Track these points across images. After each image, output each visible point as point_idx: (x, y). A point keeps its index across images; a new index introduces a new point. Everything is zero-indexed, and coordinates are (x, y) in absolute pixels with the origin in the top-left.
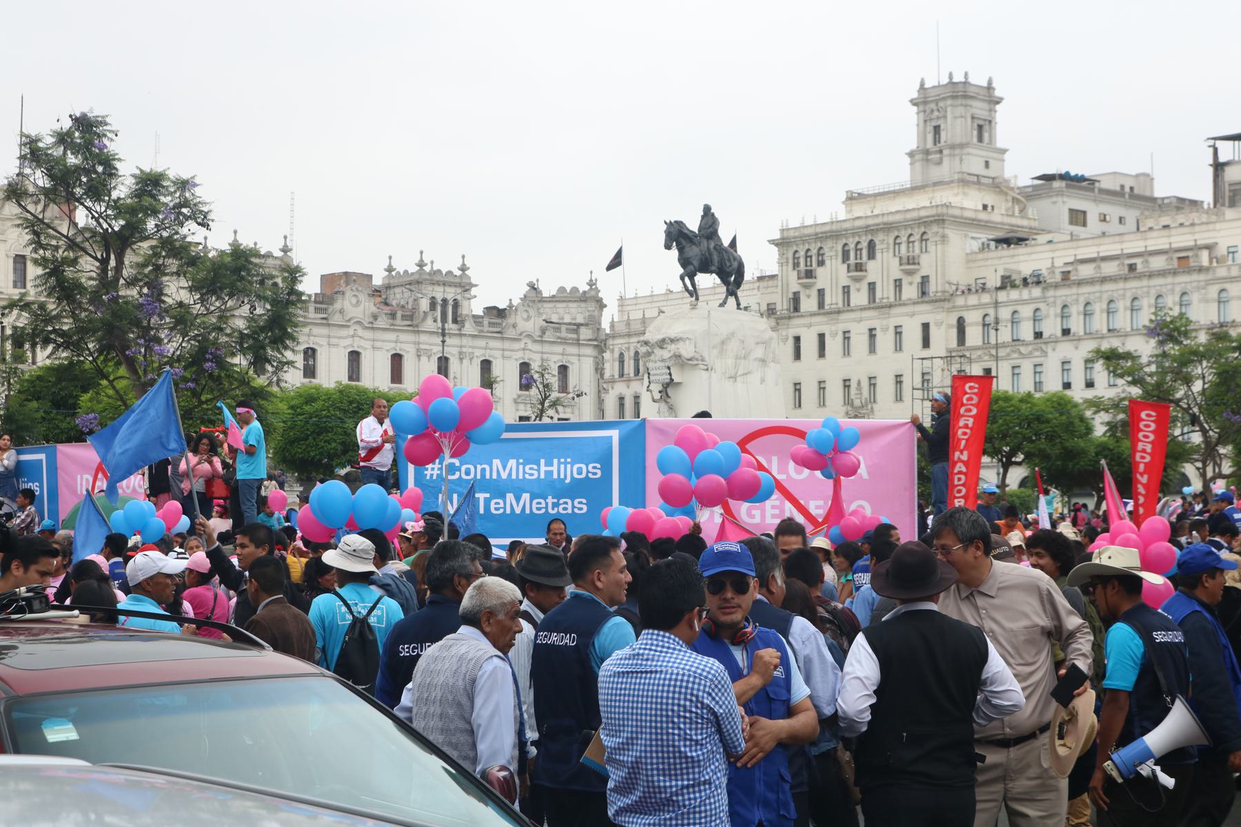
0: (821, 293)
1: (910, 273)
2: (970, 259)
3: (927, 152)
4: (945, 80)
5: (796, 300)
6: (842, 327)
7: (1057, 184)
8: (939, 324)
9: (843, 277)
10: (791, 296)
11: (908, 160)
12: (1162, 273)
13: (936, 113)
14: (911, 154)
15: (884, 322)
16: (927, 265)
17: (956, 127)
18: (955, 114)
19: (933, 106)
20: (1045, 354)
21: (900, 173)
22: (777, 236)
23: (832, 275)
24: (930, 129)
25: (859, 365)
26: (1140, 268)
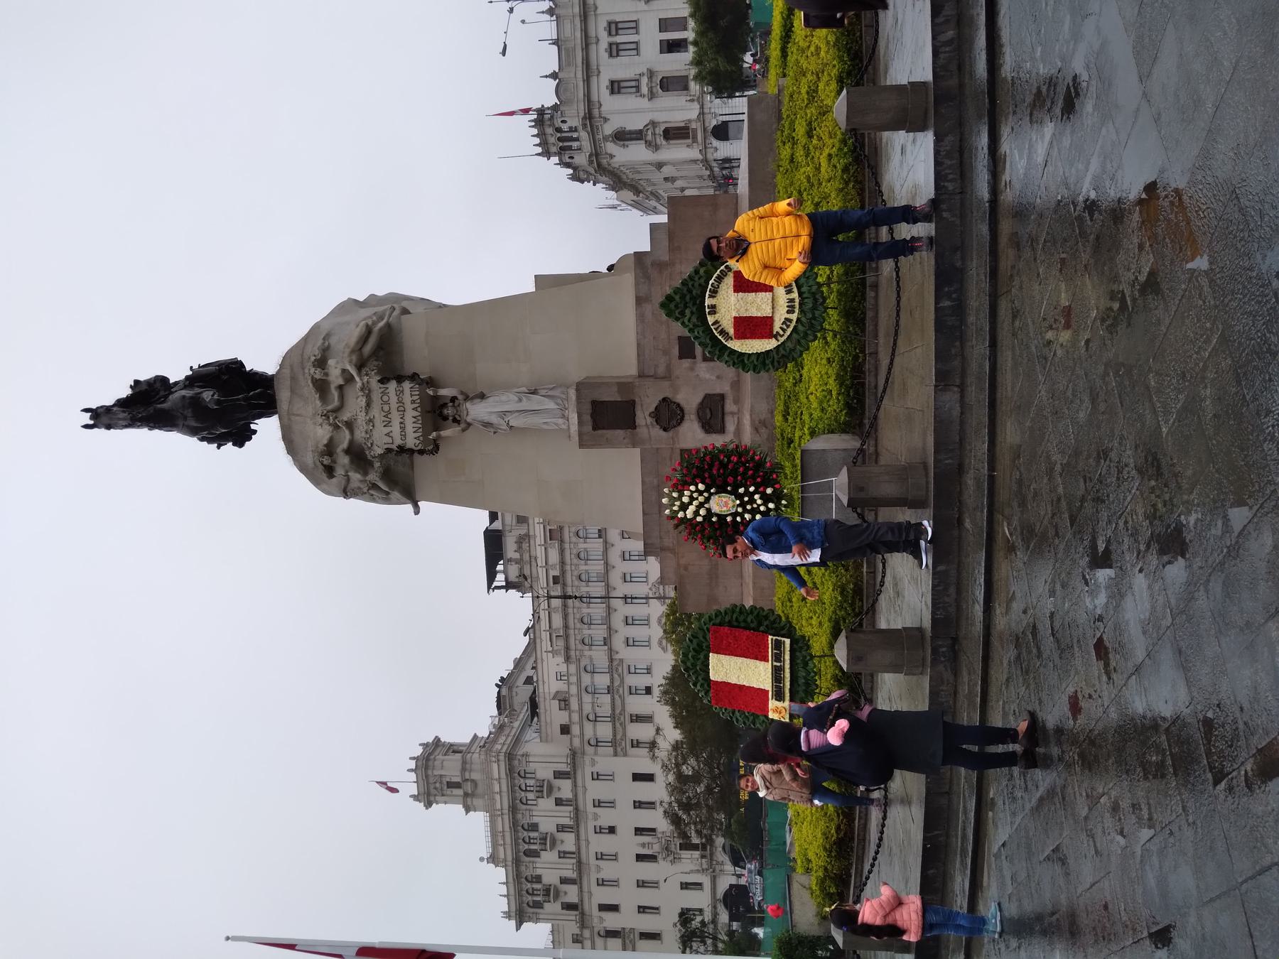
0: (564, 881)
1: (551, 789)
2: (544, 739)
3: (466, 795)
4: (413, 776)
5: (569, 907)
6: (593, 861)
7: (504, 692)
8: (593, 763)
9: (549, 856)
10: (565, 912)
11: (472, 813)
12: (562, 551)
13: (438, 785)
14: (468, 810)
15: (590, 816)
16: (545, 773)
17: (450, 768)
18: (441, 774)
19: (432, 787)
20: (621, 660)
21: (479, 819)
22: (513, 923)
23: (550, 868)
24: (449, 791)
25: (627, 844)
26: (557, 573)
